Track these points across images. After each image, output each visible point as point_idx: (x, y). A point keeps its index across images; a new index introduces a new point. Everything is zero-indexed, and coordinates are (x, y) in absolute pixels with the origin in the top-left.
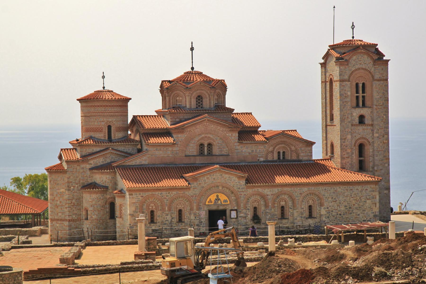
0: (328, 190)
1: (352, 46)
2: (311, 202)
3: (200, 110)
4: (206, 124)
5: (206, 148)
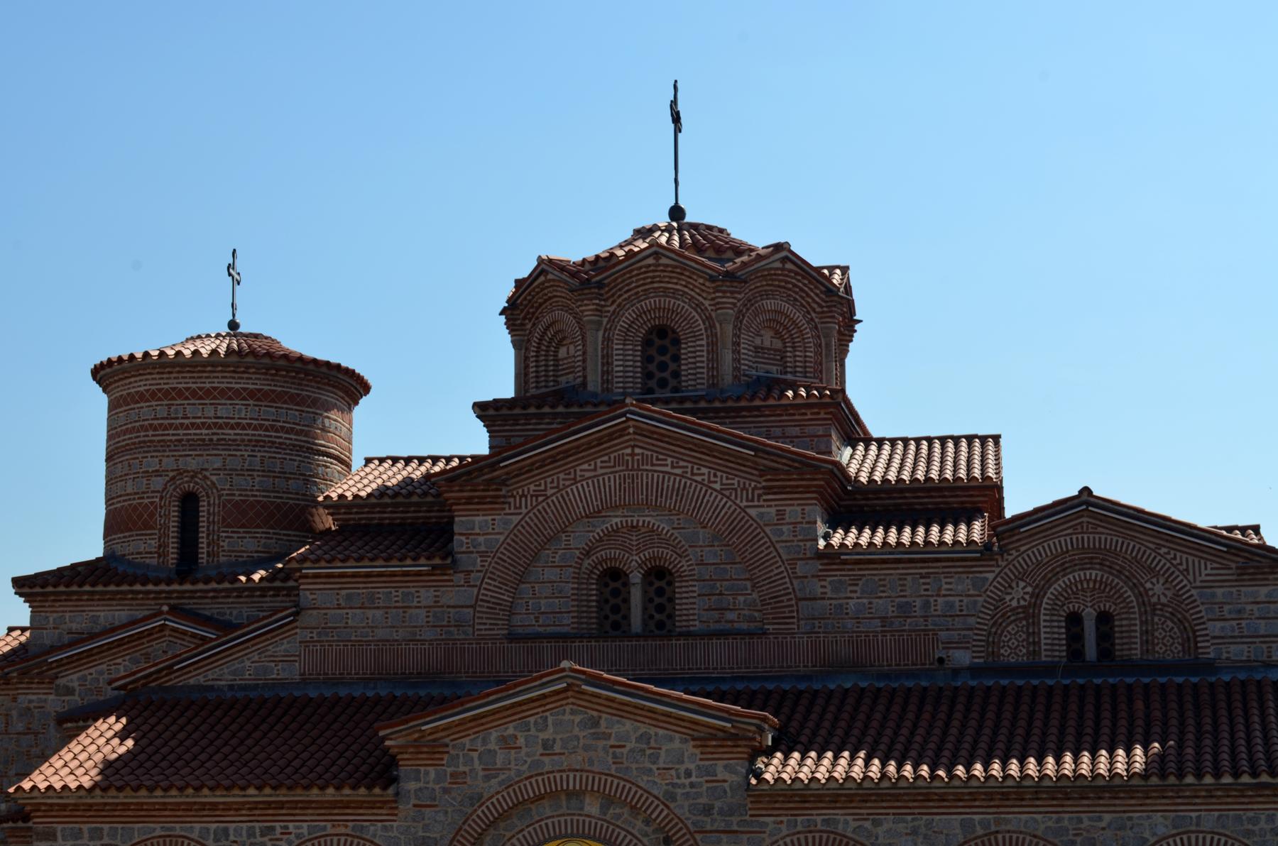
4: (633, 455)
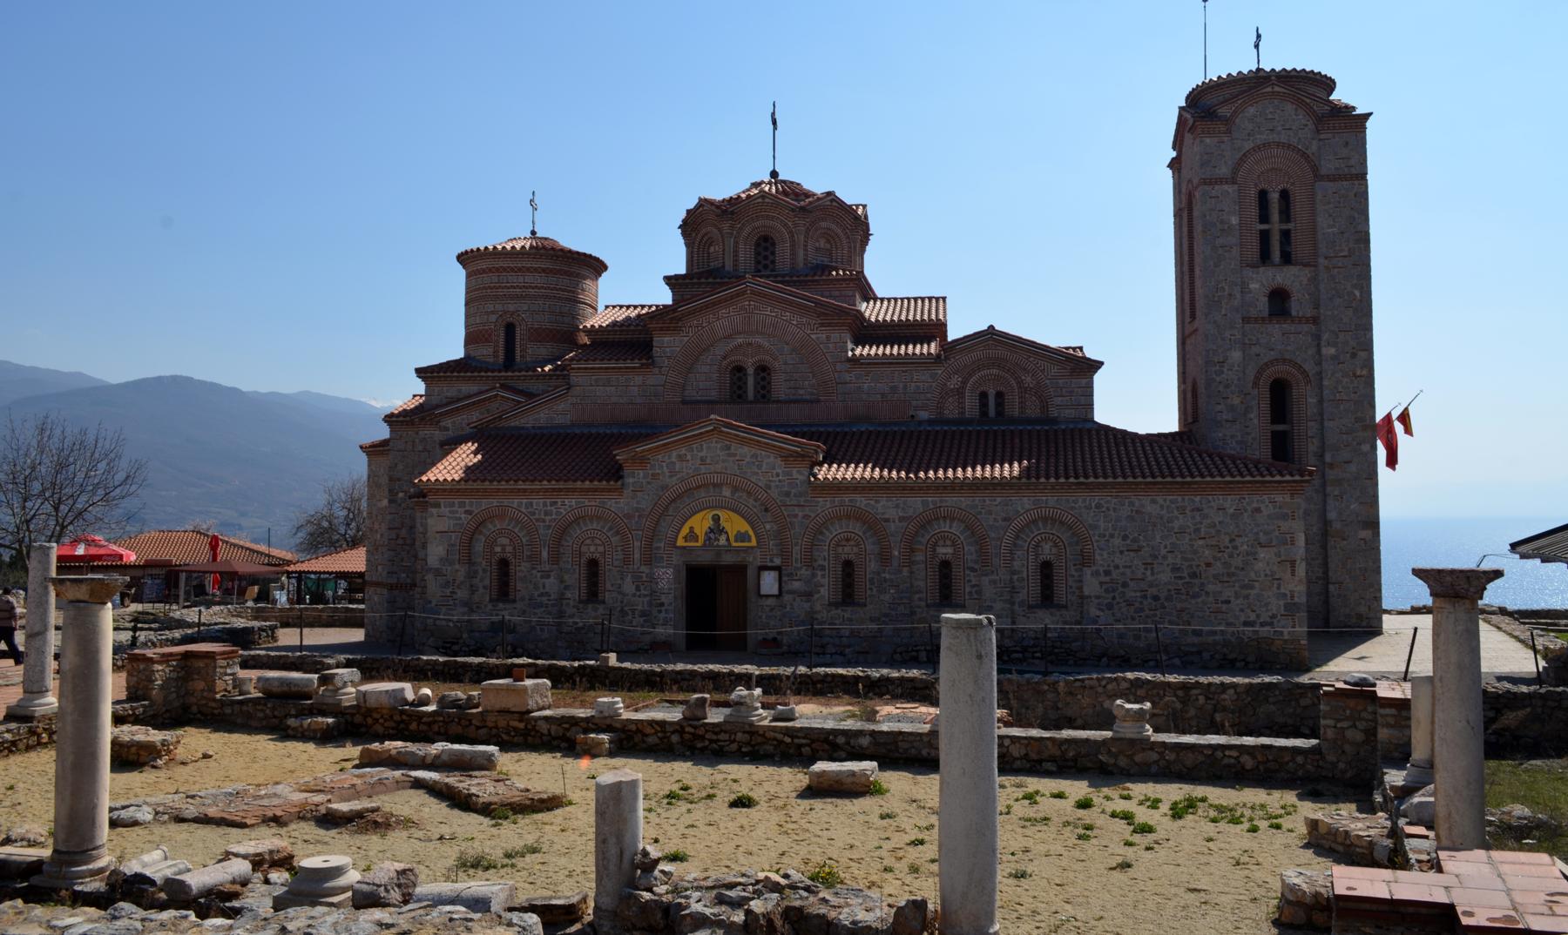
0: (1108, 509)
2: (1047, 552)
5: (751, 381)
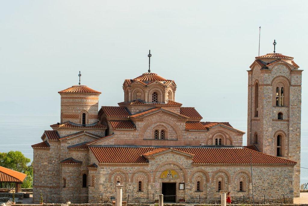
1: (274, 58)
2: (242, 180)
3: (156, 104)
5: (160, 134)
